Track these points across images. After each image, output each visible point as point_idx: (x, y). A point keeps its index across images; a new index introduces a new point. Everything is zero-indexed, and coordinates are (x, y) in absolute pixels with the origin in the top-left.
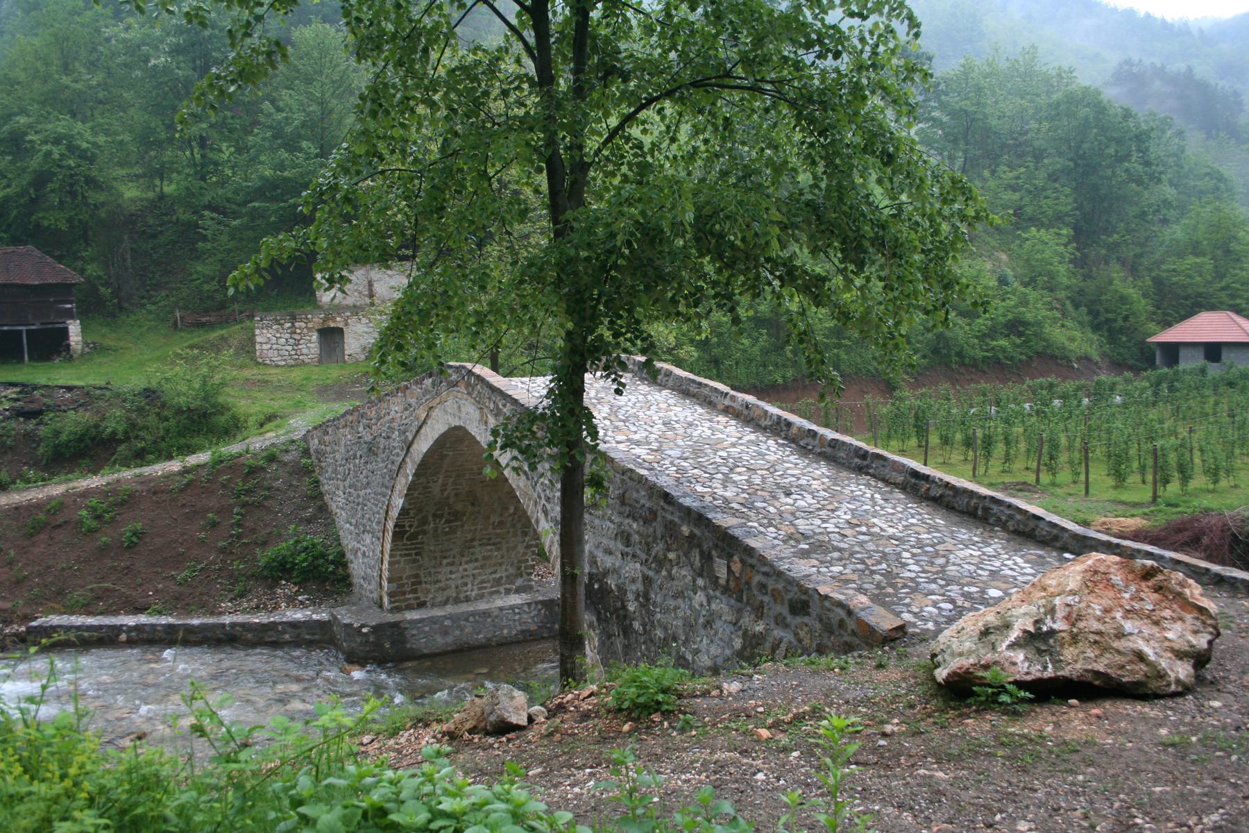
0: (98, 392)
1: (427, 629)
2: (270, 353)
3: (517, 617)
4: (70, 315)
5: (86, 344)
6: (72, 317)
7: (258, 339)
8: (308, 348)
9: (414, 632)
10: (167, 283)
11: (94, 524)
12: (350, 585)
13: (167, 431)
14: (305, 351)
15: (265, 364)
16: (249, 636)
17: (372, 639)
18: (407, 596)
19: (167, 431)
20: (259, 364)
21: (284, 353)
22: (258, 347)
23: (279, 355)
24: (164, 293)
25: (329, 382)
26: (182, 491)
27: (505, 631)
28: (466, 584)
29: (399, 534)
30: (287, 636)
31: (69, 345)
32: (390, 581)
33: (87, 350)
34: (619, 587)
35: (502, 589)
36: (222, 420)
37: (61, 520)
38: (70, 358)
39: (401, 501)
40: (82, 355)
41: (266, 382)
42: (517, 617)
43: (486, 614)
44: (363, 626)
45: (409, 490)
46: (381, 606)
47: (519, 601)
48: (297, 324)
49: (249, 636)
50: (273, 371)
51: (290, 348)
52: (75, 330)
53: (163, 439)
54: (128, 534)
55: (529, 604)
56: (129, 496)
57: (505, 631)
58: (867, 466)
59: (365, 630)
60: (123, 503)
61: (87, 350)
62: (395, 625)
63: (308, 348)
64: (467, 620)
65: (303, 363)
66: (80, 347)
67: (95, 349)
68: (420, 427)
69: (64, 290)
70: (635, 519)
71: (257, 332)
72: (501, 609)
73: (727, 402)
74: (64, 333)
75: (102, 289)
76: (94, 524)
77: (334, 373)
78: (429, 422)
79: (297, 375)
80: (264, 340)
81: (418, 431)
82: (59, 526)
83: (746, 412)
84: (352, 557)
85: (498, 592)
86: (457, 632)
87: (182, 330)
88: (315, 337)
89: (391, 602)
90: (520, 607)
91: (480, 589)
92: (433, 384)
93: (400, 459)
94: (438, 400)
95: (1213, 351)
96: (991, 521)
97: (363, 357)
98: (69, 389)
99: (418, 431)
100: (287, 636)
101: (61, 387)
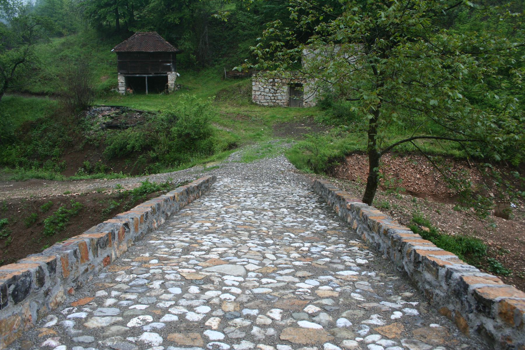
0: (150, 116)
2: (260, 98)
4: (169, 69)
5: (176, 85)
6: (170, 71)
7: (254, 88)
10: (229, 53)
13: (170, 147)
14: (279, 97)
15: (257, 104)
19: (170, 147)
20: (252, 103)
21: (266, 97)
22: (253, 93)
23: (265, 99)
24: (225, 59)
25: (286, 120)
31: (168, 85)
33: (176, 89)
36: (204, 143)
40: (174, 91)
41: (248, 116)
48: (276, 80)
50: (257, 109)
52: (172, 77)
53: (168, 152)
61: (176, 89)
65: (279, 106)
66: (173, 87)
67: (180, 88)
69: (165, 56)
71: (253, 83)
74: (166, 79)
75: (192, 56)
77: (293, 114)
79: (269, 113)
80: (257, 89)
87: (227, 80)
88: (286, 88)
97: (314, 104)
98: (141, 113)
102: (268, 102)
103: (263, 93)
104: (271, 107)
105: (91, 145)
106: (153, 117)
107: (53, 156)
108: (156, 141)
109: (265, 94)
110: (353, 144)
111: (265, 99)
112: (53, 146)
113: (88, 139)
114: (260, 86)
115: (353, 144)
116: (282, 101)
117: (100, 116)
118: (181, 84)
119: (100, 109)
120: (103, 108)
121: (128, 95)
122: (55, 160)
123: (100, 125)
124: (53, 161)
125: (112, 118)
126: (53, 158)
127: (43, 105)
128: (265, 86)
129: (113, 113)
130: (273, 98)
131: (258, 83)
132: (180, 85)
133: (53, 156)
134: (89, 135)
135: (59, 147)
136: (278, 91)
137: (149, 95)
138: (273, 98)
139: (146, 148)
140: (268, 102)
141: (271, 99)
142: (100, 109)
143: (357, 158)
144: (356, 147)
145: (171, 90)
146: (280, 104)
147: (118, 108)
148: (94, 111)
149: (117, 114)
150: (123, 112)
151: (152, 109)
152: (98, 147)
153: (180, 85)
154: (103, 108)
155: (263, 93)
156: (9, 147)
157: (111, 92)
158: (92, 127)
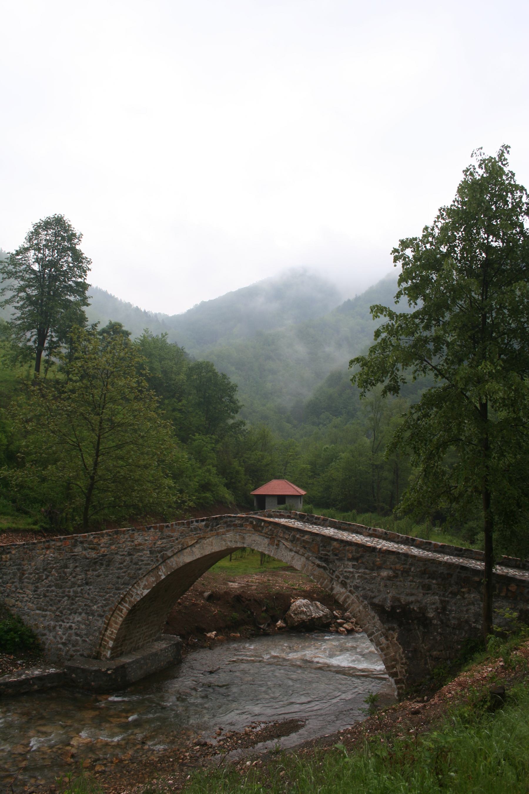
1: (134, 667)
3: (166, 654)
9: (130, 670)
12: (43, 650)
16: (10, 691)
17: (114, 677)
18: (118, 649)
27: (162, 663)
28: (140, 639)
29: (132, 612)
30: (36, 687)
32: (115, 640)
34: (420, 608)
35: (151, 640)
39: (146, 592)
42: (166, 654)
43: (156, 654)
44: (108, 669)
45: (158, 584)
46: (97, 657)
47: (164, 646)
49: (10, 691)
55: (171, 646)
57: (162, 663)
58: (463, 554)
59: (109, 672)
62: (123, 667)
64: (149, 659)
68: (183, 549)
70: (433, 578)
72: (161, 650)
73: (371, 532)
78: (197, 546)
81: (179, 551)
83: (385, 536)
84: (46, 632)
85: (149, 642)
86: (145, 667)
89: (111, 654)
90: (166, 648)
91: (144, 640)
92: (207, 526)
93: (150, 568)
94: (214, 532)
95: (281, 499)
96: (527, 568)
99: (179, 551)
100: (36, 687)
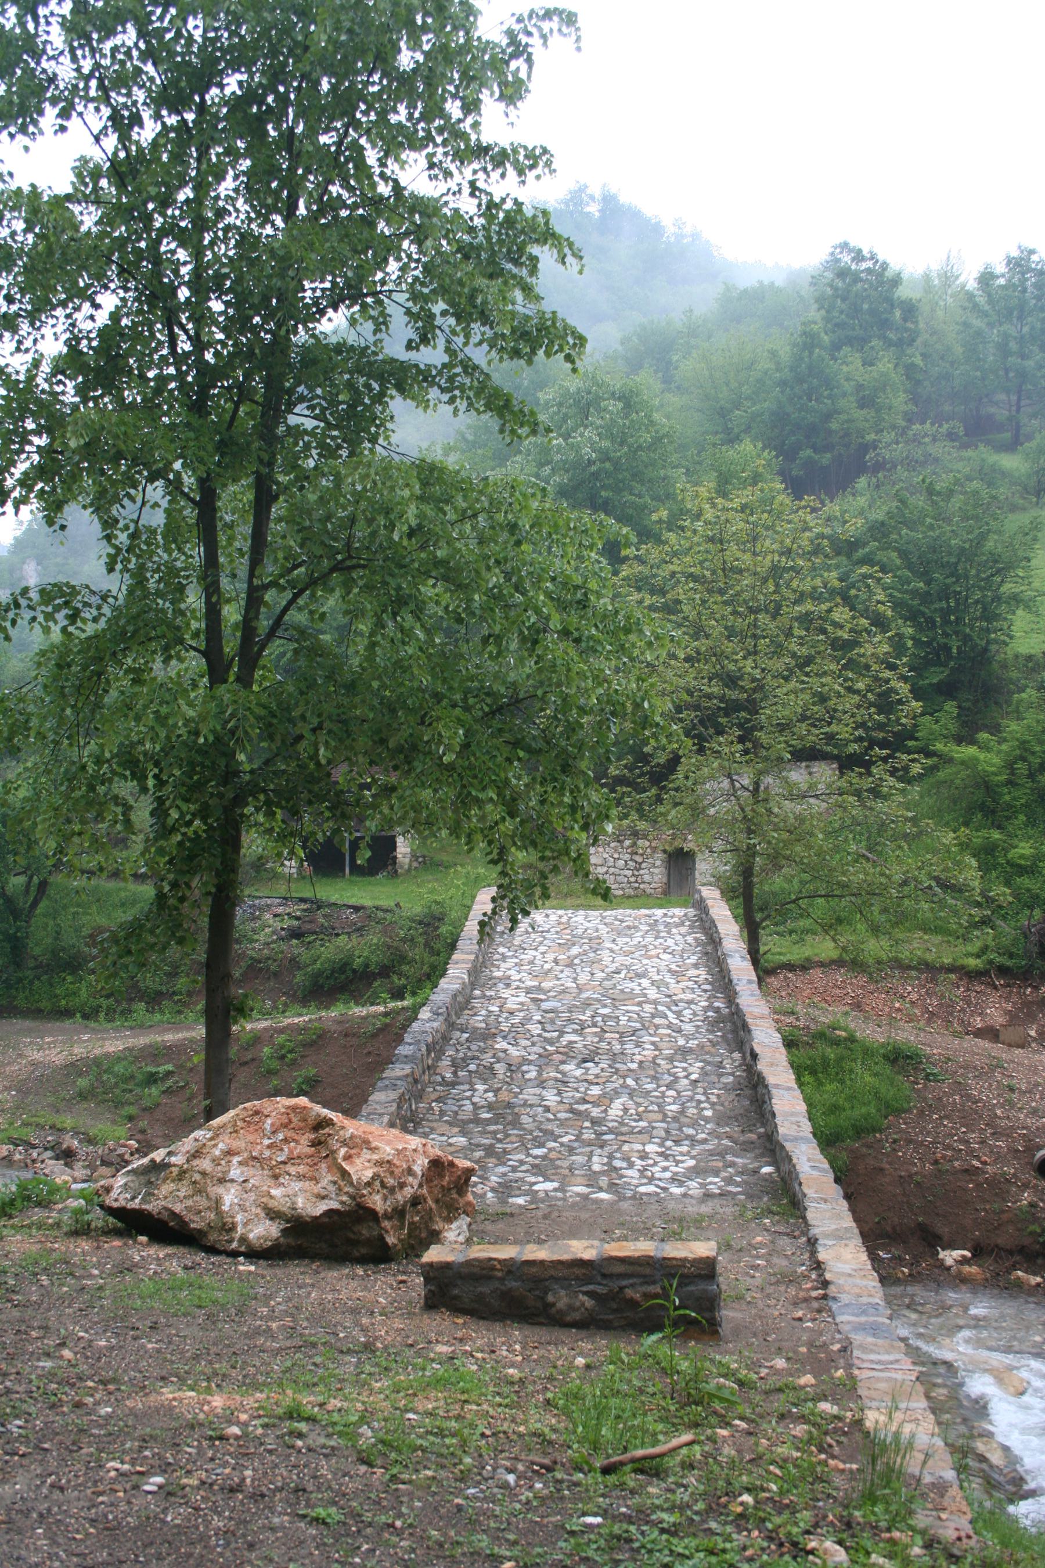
0: (380, 914)
5: (414, 856)
7: (593, 860)
8: (652, 874)
11: (275, 1064)
14: (647, 878)
23: (616, 882)
26: (374, 1036)
31: (395, 857)
33: (415, 864)
37: (250, 1057)
38: (395, 874)
40: (409, 870)
51: (629, 873)
54: (300, 1080)
56: (320, 1037)
60: (312, 1044)
61: (415, 864)
63: (652, 874)
66: (407, 860)
67: (426, 863)
76: (275, 1064)
80: (599, 861)
82: (246, 1063)
88: (659, 859)
98: (357, 909)
101: (349, 907)
102: (623, 889)
103: (612, 870)
104: (629, 897)
105: (261, 969)
106: (388, 916)
107: (174, 993)
108: (403, 959)
109: (617, 871)
110: (780, 954)
111: (616, 882)
112: (173, 974)
113: (252, 958)
114: (606, 856)
115: (780, 954)
116: (653, 886)
117: (268, 916)
118: (426, 853)
119: (264, 901)
120: (269, 901)
121: (304, 878)
122: (180, 1001)
123: (274, 933)
124: (176, 1003)
125: (298, 918)
126: (176, 998)
127: (123, 894)
128: (616, 856)
129: (297, 909)
130: (632, 879)
131: (601, 849)
132: (424, 857)
133: (174, 993)
134: (254, 949)
135: (188, 975)
136: (644, 865)
137: (354, 878)
138: (632, 879)
139: (385, 971)
140: (623, 889)
141: (629, 882)
142: (264, 901)
143: (786, 978)
144: (784, 959)
145: (402, 867)
146: (649, 891)
147: (303, 900)
148: (250, 907)
149: (305, 910)
150: (319, 908)
151: (384, 903)
152: (276, 974)
153: (424, 857)
154: (269, 901)
155: (612, 870)
156: (69, 979)
157: (266, 870)
158: (256, 937)
